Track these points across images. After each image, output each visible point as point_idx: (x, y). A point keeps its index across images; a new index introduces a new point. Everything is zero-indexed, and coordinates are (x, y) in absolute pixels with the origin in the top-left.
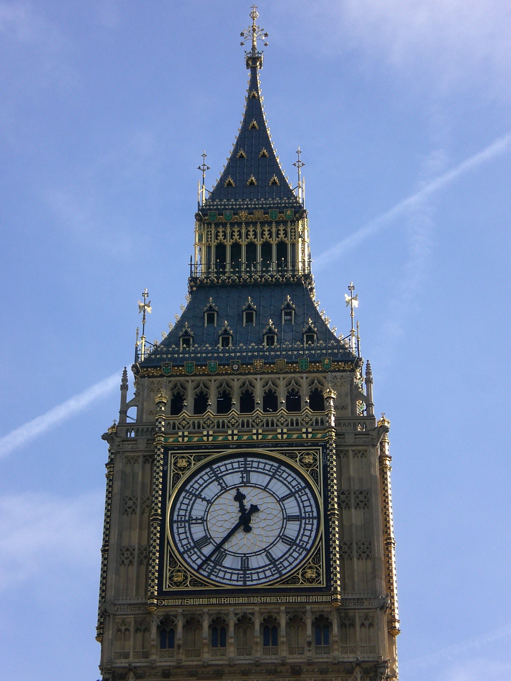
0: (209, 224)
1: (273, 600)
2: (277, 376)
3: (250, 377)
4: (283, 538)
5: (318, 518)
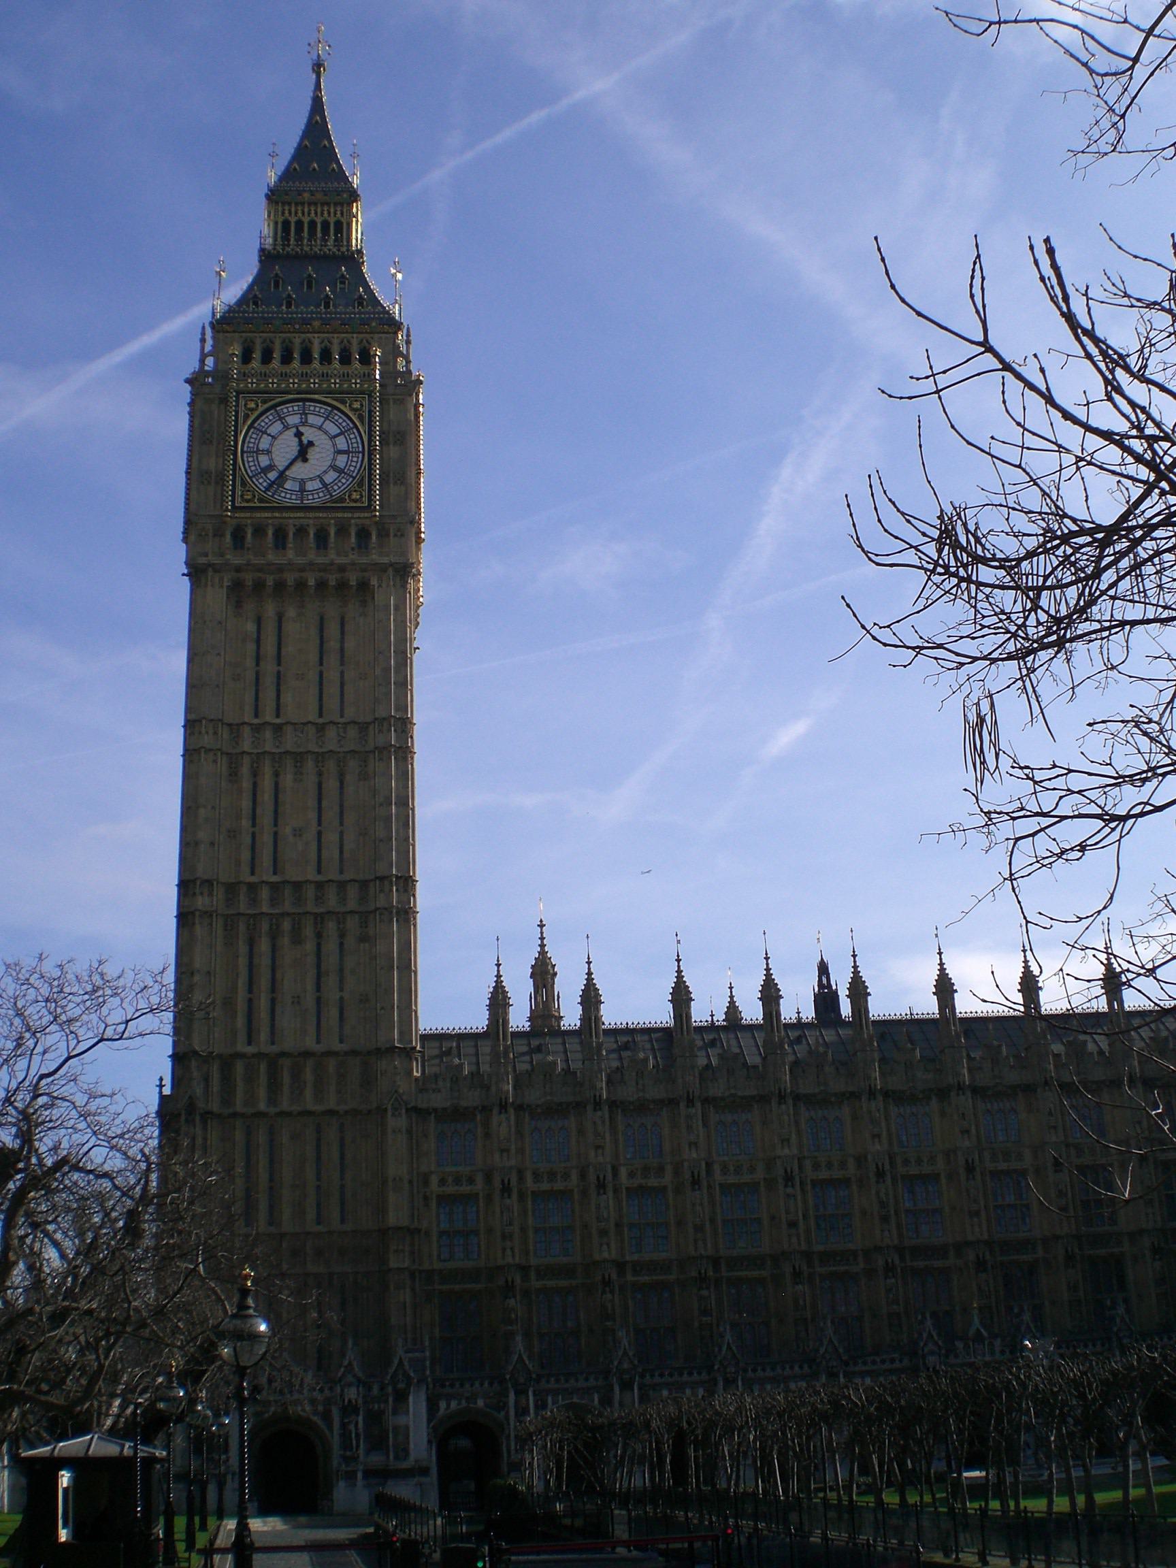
0: (277, 203)
1: (325, 515)
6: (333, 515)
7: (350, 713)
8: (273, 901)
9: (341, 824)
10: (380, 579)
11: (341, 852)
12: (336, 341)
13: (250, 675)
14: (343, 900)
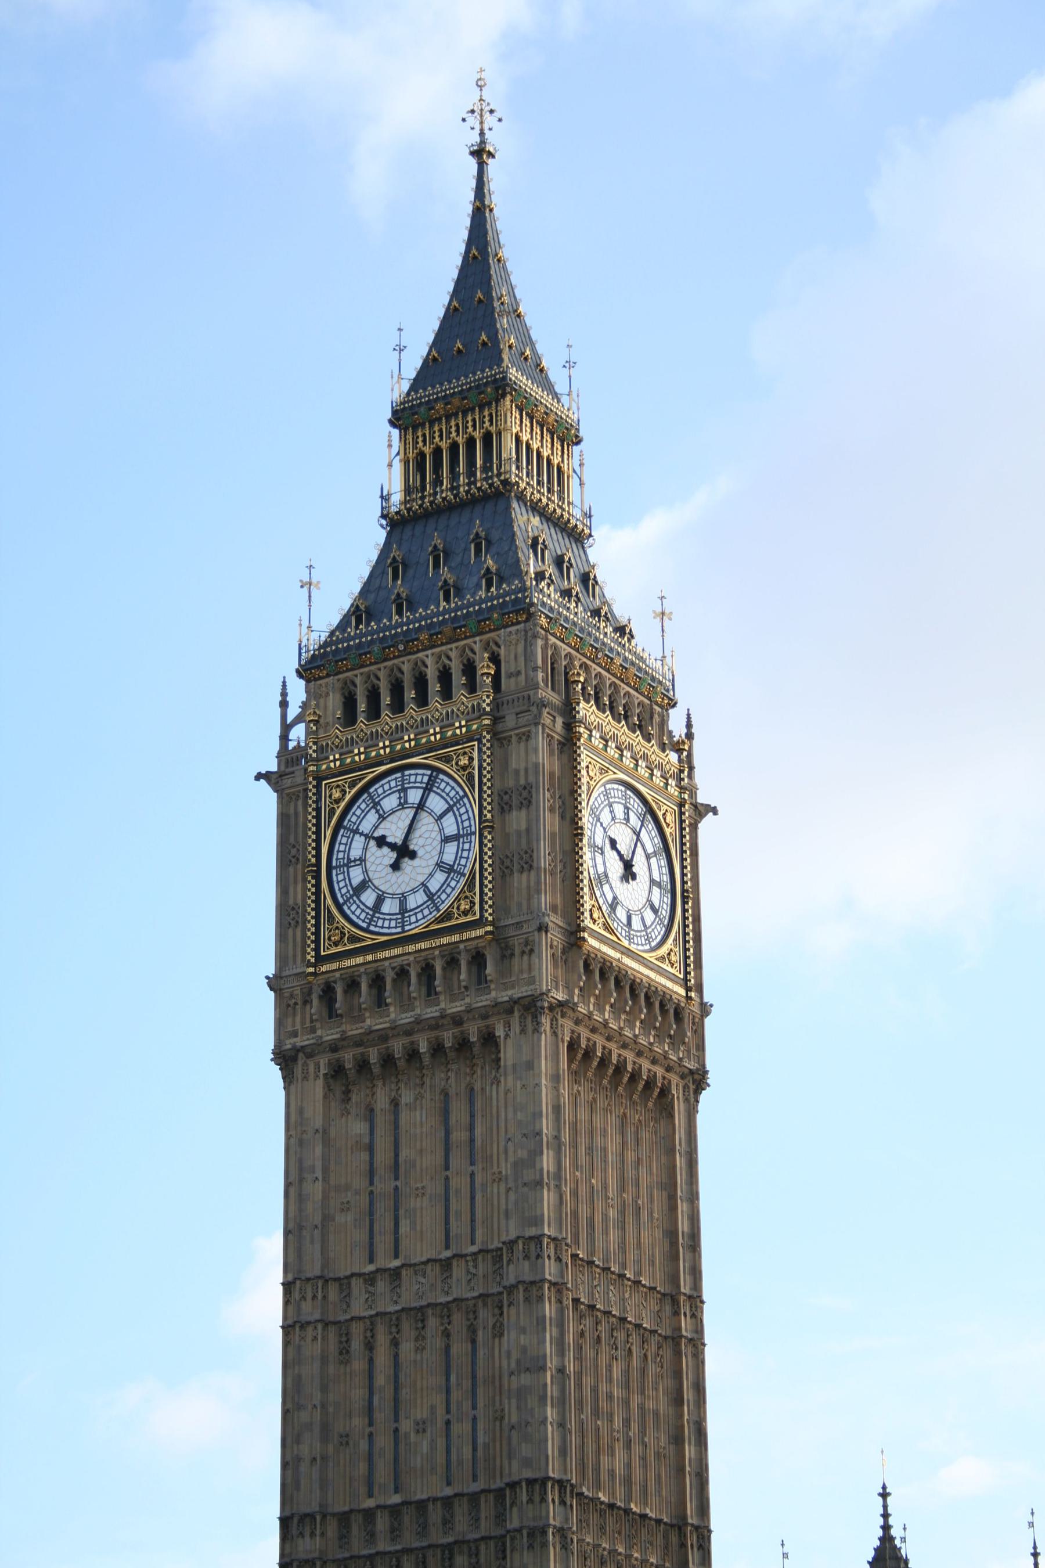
0: (406, 429)
2: (449, 646)
3: (420, 655)
4: (440, 865)
5: (475, 833)
6: (437, 942)
8: (395, 1532)
9: (474, 1407)
10: (508, 1025)
11: (475, 1450)
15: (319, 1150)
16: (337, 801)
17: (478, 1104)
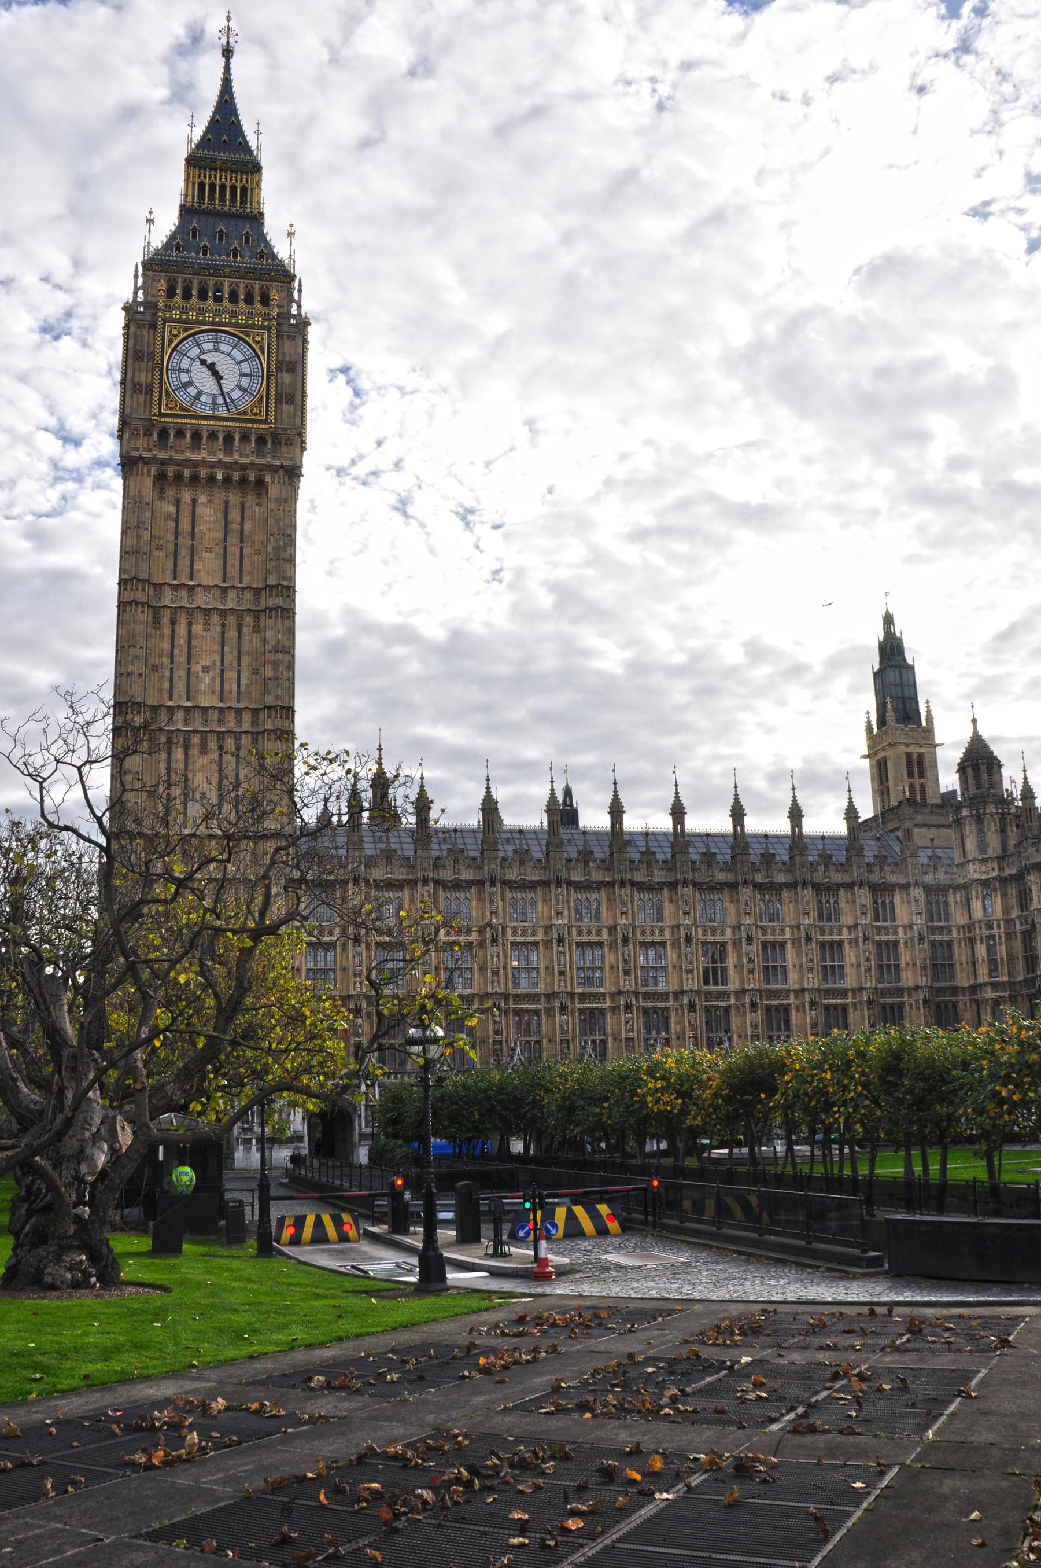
7: (247, 579)
10: (273, 478)
11: (239, 686)
12: (242, 285)
13: (171, 547)
14: (239, 722)
15: (148, 514)
16: (175, 336)
17: (248, 513)
